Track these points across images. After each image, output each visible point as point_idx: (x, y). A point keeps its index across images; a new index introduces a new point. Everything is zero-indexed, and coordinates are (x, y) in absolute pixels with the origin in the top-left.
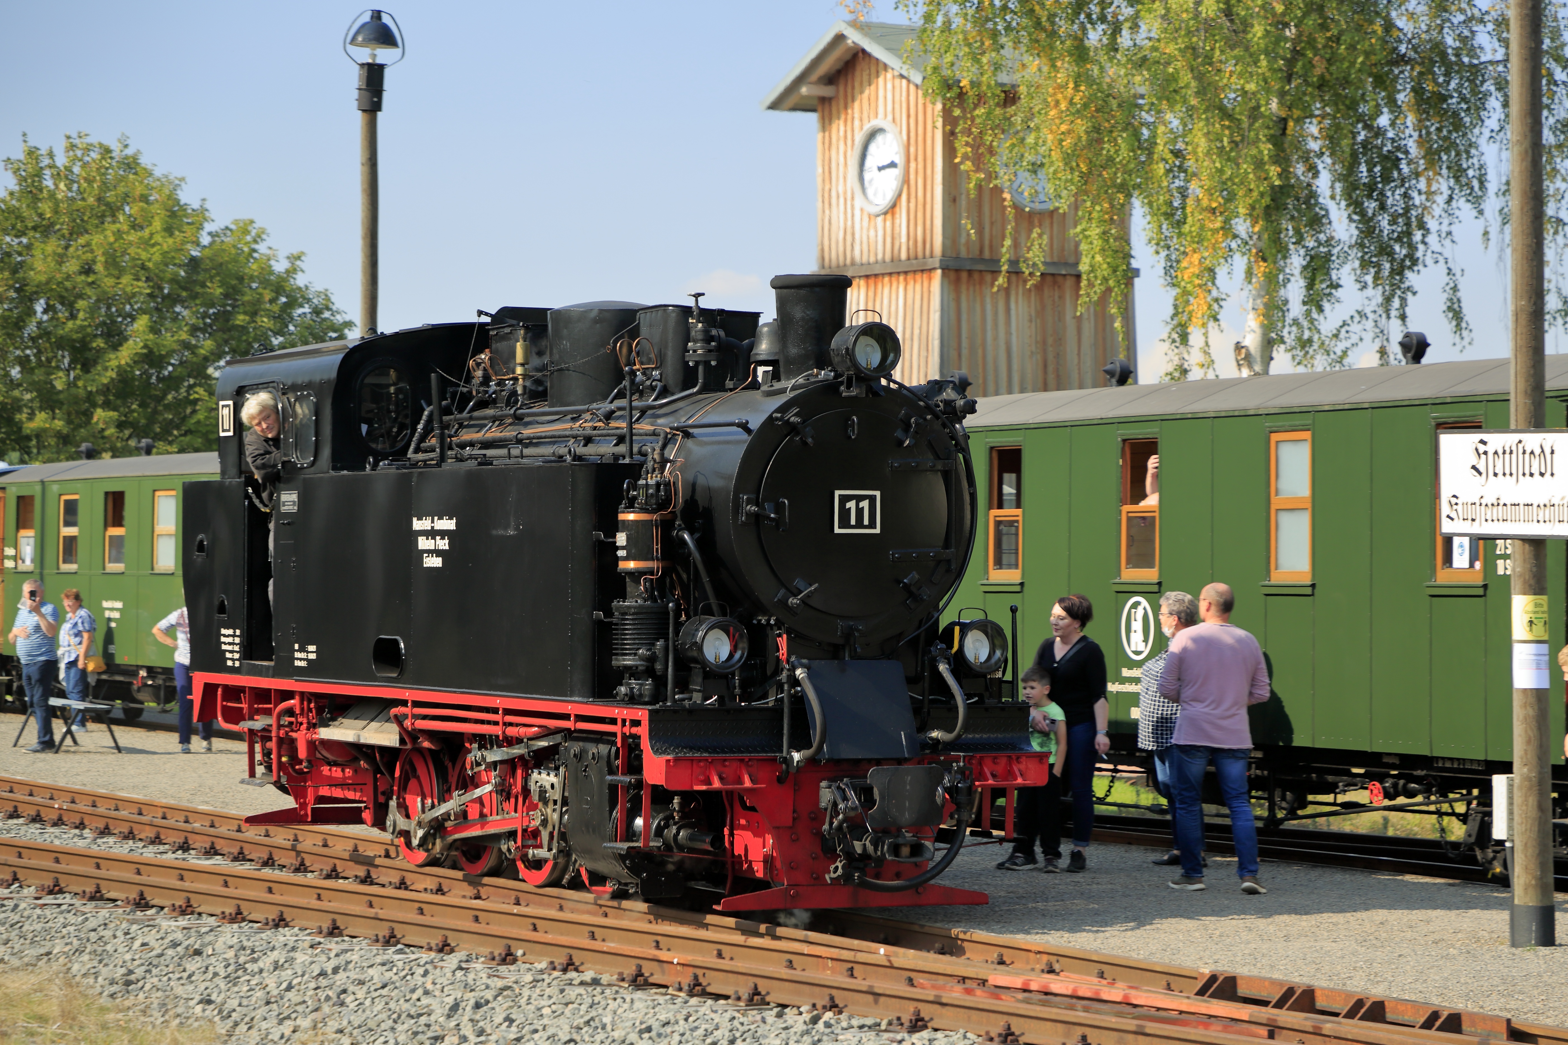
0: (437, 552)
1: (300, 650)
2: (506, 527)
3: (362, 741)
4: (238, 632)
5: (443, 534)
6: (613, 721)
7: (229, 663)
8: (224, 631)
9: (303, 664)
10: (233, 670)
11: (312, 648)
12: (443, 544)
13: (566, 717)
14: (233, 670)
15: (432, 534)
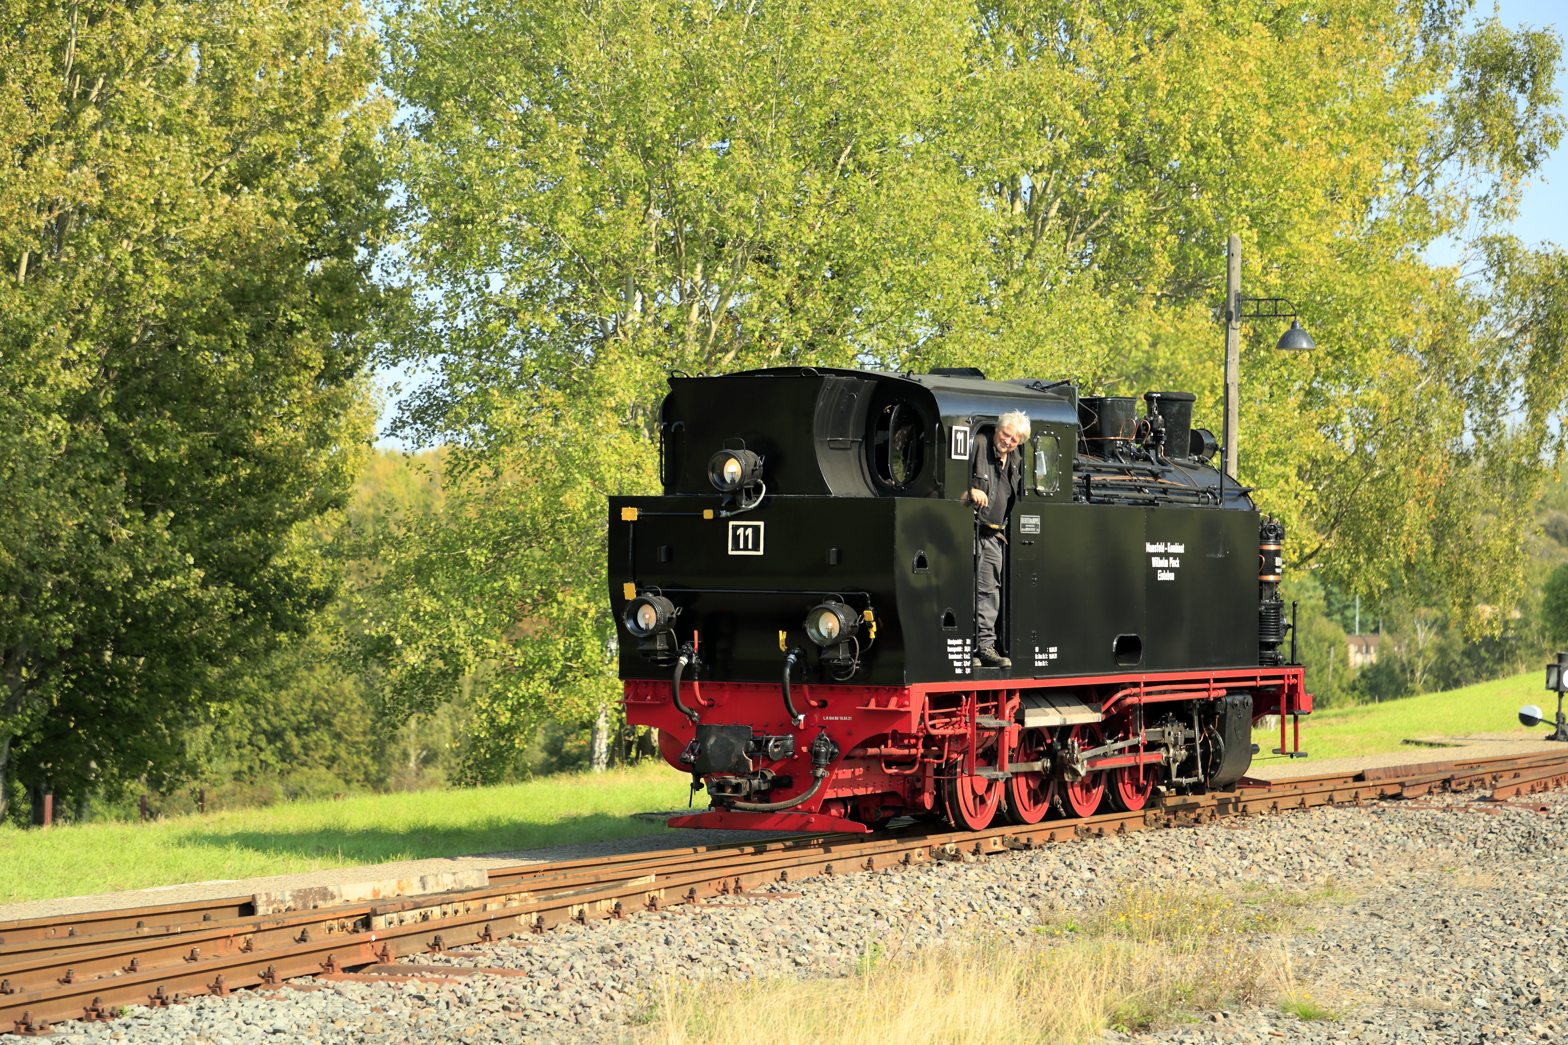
0: (1170, 569)
1: (1041, 652)
2: (1217, 552)
3: (1068, 722)
4: (968, 641)
5: (1175, 556)
6: (1281, 677)
7: (958, 671)
8: (950, 642)
9: (1044, 664)
10: (963, 677)
11: (1053, 649)
12: (1175, 563)
13: (1253, 679)
14: (963, 677)
15: (1166, 555)
